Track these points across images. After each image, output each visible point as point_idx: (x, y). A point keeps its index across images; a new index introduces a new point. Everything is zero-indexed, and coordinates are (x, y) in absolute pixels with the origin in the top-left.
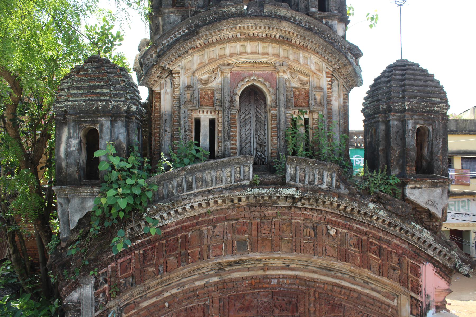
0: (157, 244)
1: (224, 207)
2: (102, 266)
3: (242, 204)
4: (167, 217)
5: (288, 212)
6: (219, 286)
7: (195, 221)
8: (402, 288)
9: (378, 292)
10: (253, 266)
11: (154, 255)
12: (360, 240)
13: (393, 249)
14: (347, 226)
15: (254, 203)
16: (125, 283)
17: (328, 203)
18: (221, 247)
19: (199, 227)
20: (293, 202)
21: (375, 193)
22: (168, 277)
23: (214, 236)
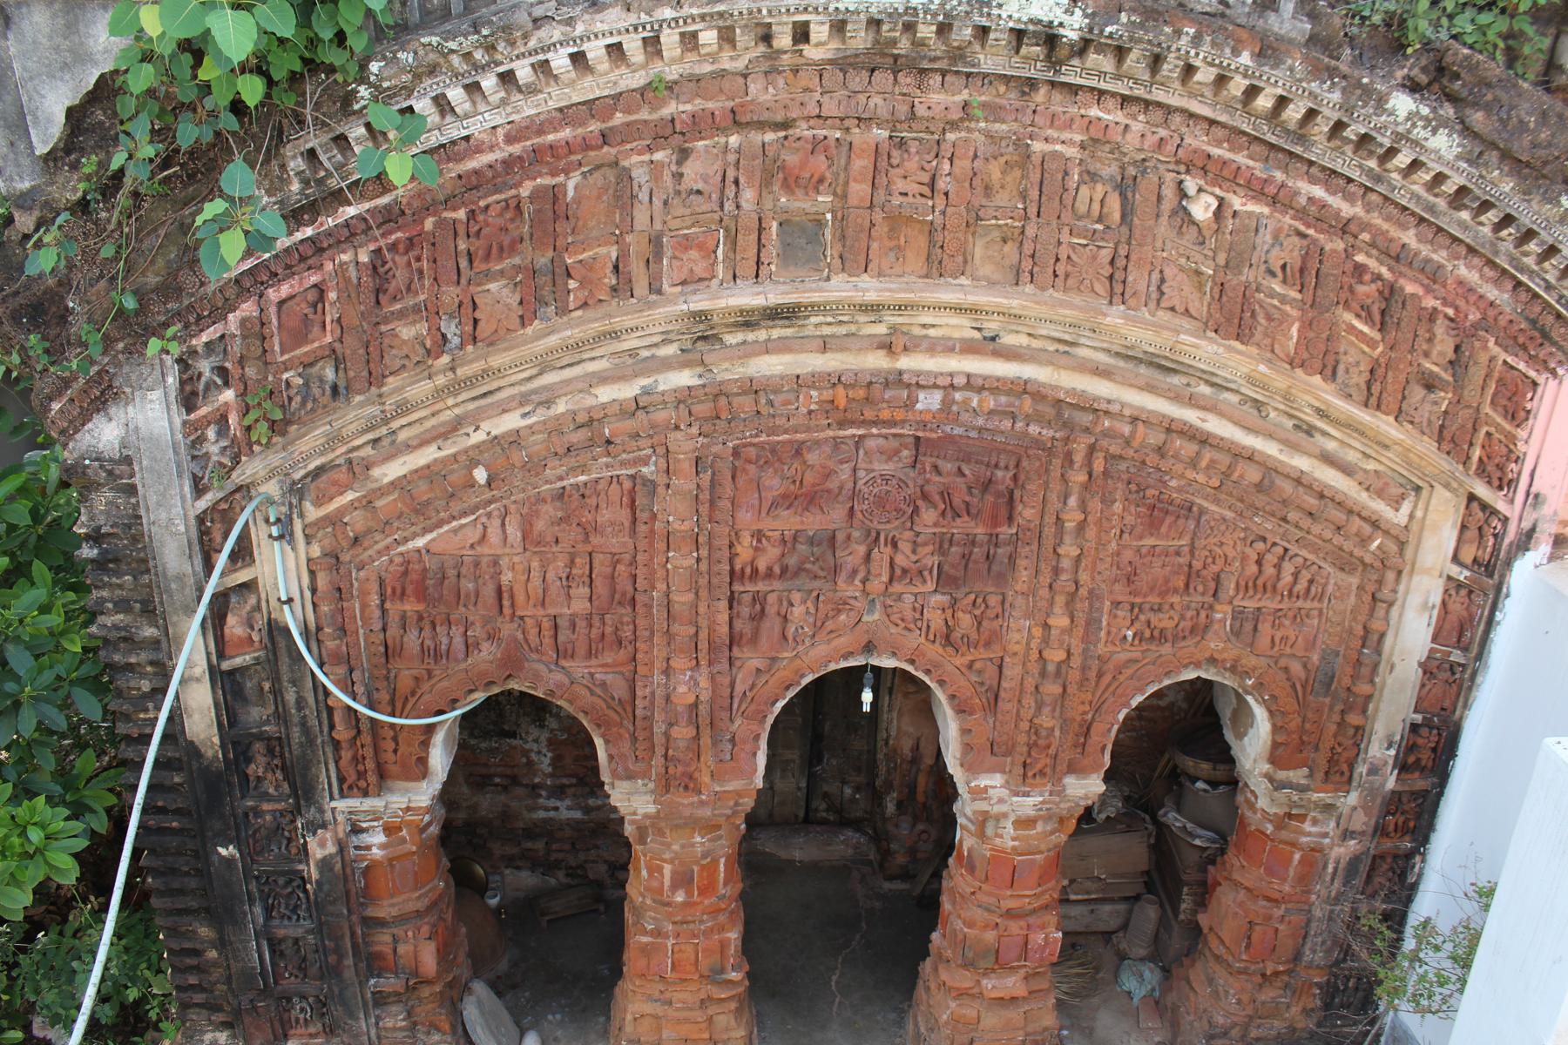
0: (429, 224)
1: (727, 65)
2: (199, 318)
3: (812, 52)
4: (467, 106)
5: (1018, 104)
6: (696, 409)
7: (594, 127)
8: (1445, 464)
9: (1346, 470)
10: (843, 330)
11: (421, 272)
12: (1313, 253)
13: (1445, 303)
14: (1271, 190)
15: (868, 53)
16: (307, 384)
17: (1205, 75)
18: (711, 244)
19: (613, 151)
20: (1049, 57)
21: (1427, 45)
22: (477, 367)
23: (678, 193)
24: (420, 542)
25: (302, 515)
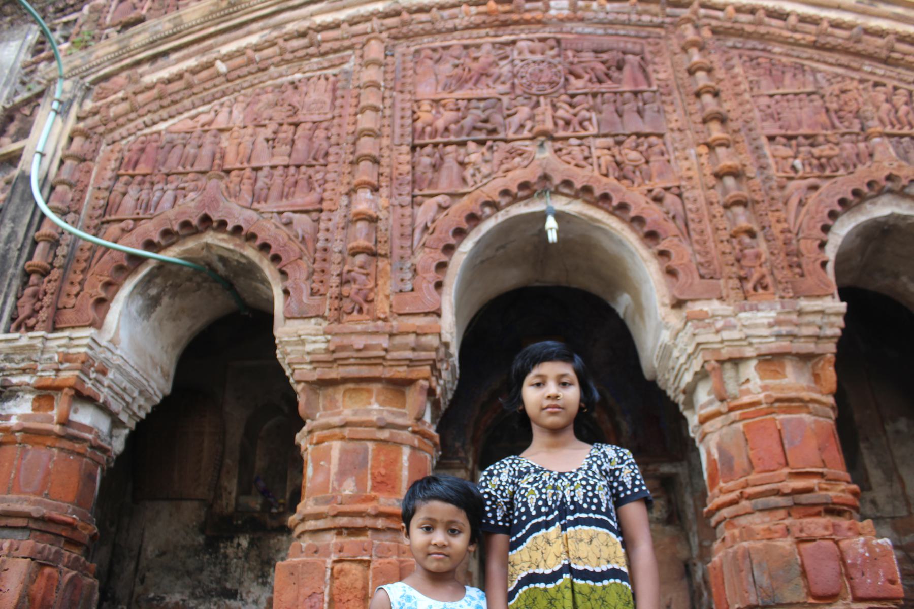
24: (162, 126)
25: (81, 105)
